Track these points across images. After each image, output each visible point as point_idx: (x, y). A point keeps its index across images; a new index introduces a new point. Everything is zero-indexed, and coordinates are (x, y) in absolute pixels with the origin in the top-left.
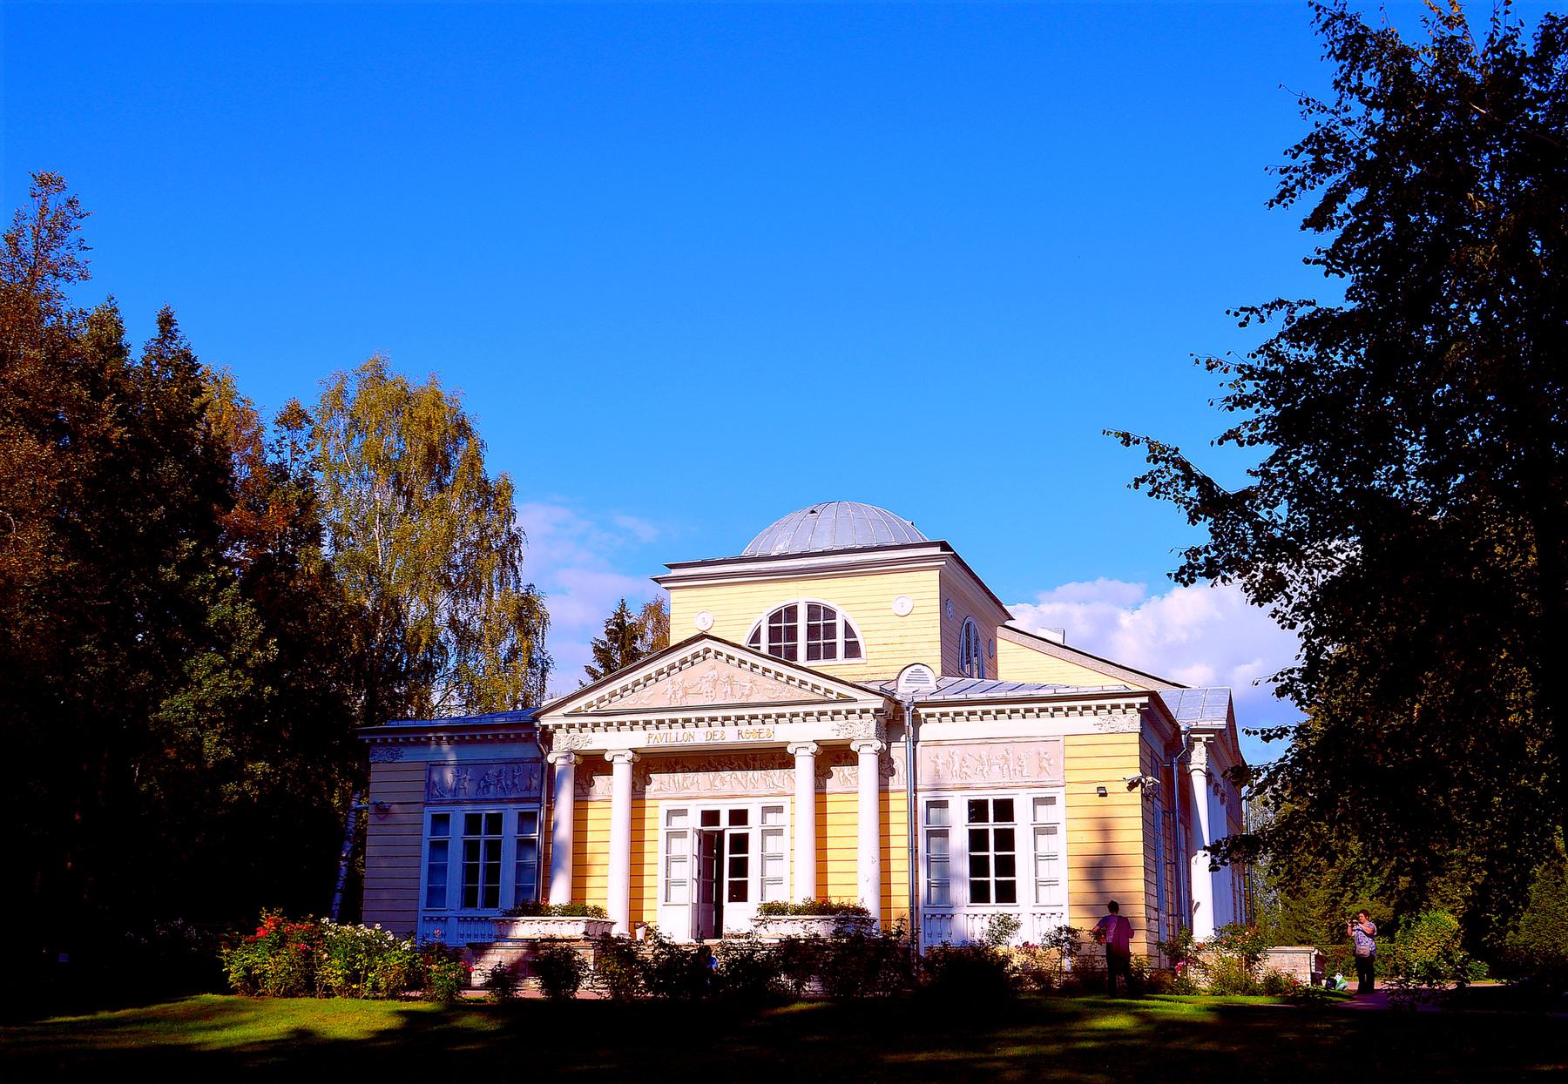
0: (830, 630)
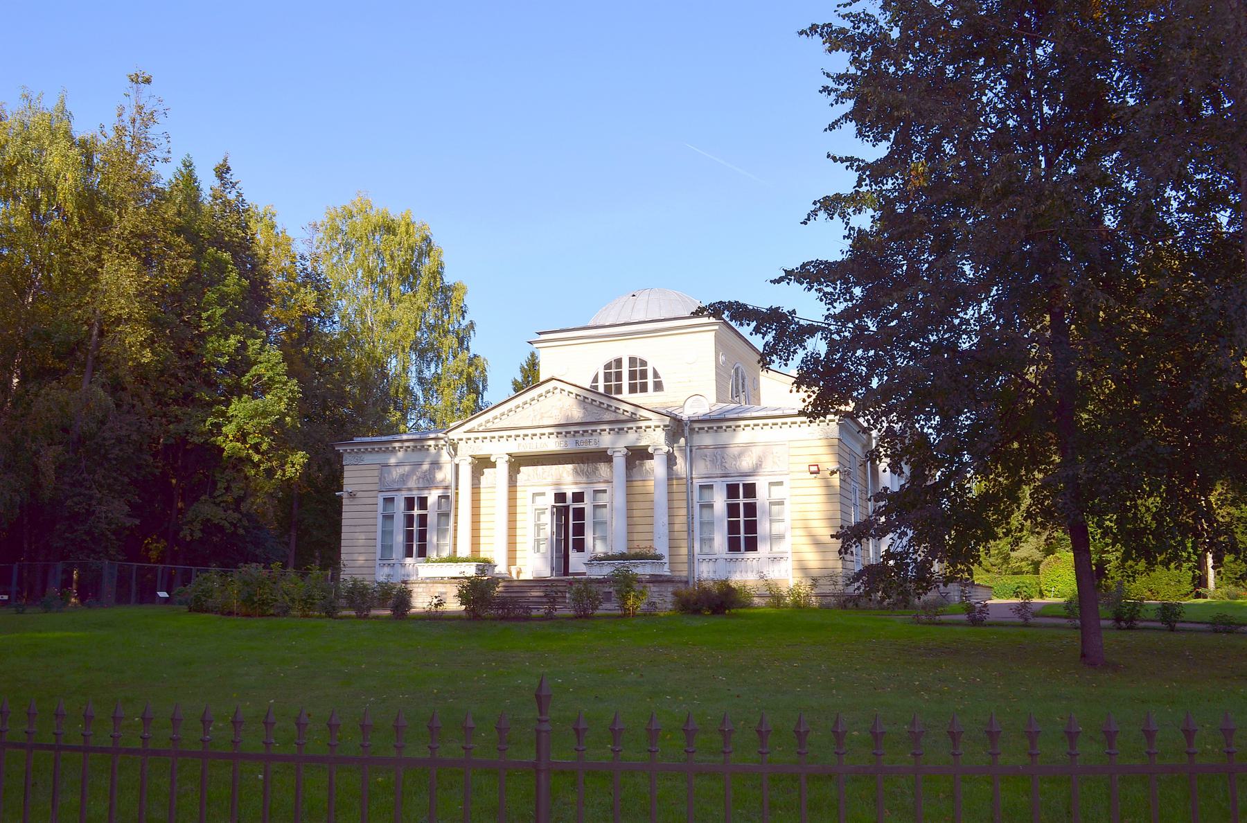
0: (644, 374)
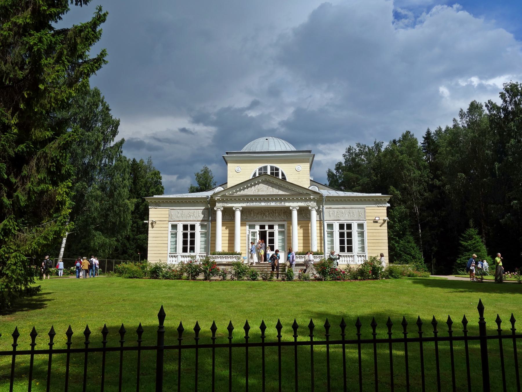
0: (277, 174)
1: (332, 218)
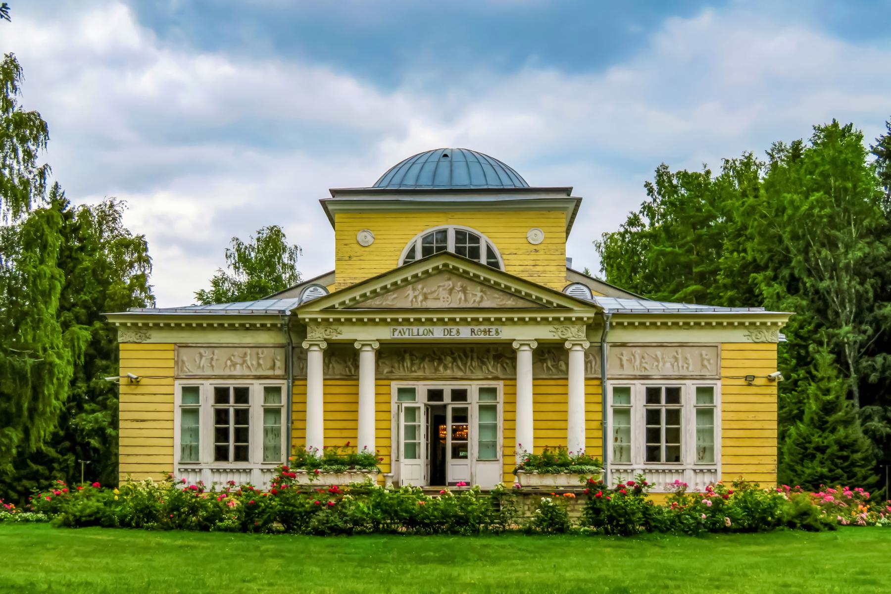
0: (475, 252)
1: (628, 371)
